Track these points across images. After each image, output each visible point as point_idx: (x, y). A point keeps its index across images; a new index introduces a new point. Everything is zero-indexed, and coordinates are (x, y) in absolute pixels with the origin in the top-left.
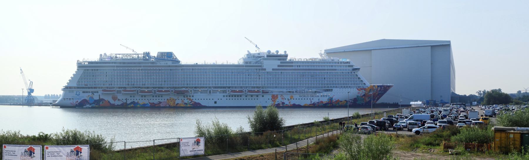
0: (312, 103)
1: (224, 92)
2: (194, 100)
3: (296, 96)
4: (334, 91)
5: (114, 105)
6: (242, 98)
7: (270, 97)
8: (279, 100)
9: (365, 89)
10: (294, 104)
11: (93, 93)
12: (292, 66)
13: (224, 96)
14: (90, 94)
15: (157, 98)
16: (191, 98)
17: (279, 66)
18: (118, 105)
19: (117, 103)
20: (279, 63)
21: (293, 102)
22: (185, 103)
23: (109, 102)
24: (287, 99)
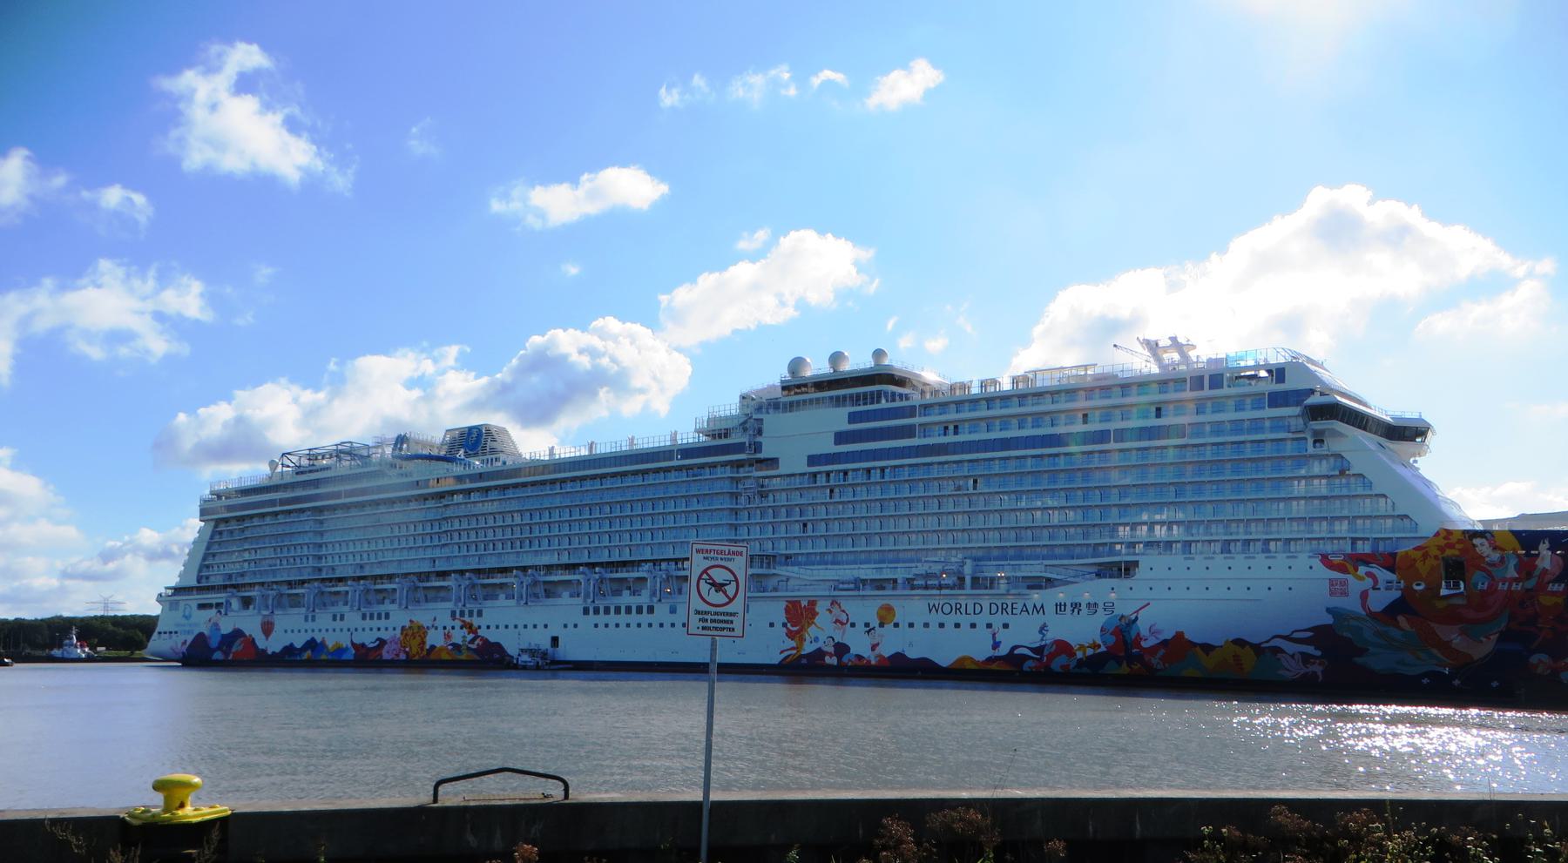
0: (1003, 650)
2: (480, 632)
3: (912, 608)
4: (1141, 572)
6: (655, 618)
7: (781, 617)
8: (821, 634)
9: (1390, 561)
10: (899, 657)
12: (908, 432)
14: (214, 611)
15: (375, 623)
16: (476, 621)
17: (841, 438)
19: (273, 645)
20: (839, 418)
21: (891, 643)
22: (456, 647)
24: (860, 627)
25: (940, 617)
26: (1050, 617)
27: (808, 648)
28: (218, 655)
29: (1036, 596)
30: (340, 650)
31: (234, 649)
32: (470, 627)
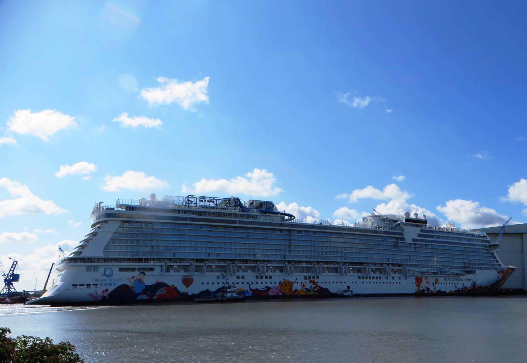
0: (457, 289)
1: (359, 271)
2: (318, 284)
3: (441, 280)
5: (185, 294)
6: (381, 281)
7: (414, 281)
8: (423, 285)
10: (439, 291)
11: (143, 271)
13: (359, 278)
14: (136, 273)
15: (264, 280)
18: (193, 295)
19: (194, 289)
22: (307, 290)
23: (176, 288)
24: (431, 284)
25: (447, 282)
26: (464, 282)
27: (421, 289)
28: (144, 297)
29: (462, 277)
30: (242, 292)
31: (158, 293)
32: (314, 283)
